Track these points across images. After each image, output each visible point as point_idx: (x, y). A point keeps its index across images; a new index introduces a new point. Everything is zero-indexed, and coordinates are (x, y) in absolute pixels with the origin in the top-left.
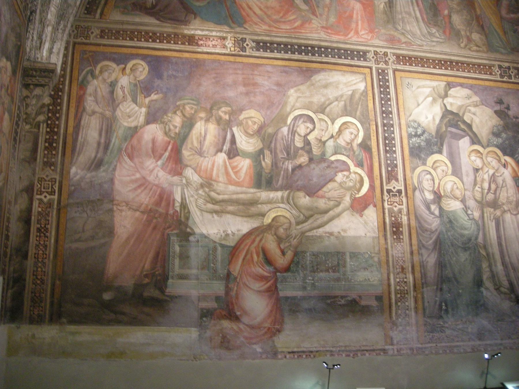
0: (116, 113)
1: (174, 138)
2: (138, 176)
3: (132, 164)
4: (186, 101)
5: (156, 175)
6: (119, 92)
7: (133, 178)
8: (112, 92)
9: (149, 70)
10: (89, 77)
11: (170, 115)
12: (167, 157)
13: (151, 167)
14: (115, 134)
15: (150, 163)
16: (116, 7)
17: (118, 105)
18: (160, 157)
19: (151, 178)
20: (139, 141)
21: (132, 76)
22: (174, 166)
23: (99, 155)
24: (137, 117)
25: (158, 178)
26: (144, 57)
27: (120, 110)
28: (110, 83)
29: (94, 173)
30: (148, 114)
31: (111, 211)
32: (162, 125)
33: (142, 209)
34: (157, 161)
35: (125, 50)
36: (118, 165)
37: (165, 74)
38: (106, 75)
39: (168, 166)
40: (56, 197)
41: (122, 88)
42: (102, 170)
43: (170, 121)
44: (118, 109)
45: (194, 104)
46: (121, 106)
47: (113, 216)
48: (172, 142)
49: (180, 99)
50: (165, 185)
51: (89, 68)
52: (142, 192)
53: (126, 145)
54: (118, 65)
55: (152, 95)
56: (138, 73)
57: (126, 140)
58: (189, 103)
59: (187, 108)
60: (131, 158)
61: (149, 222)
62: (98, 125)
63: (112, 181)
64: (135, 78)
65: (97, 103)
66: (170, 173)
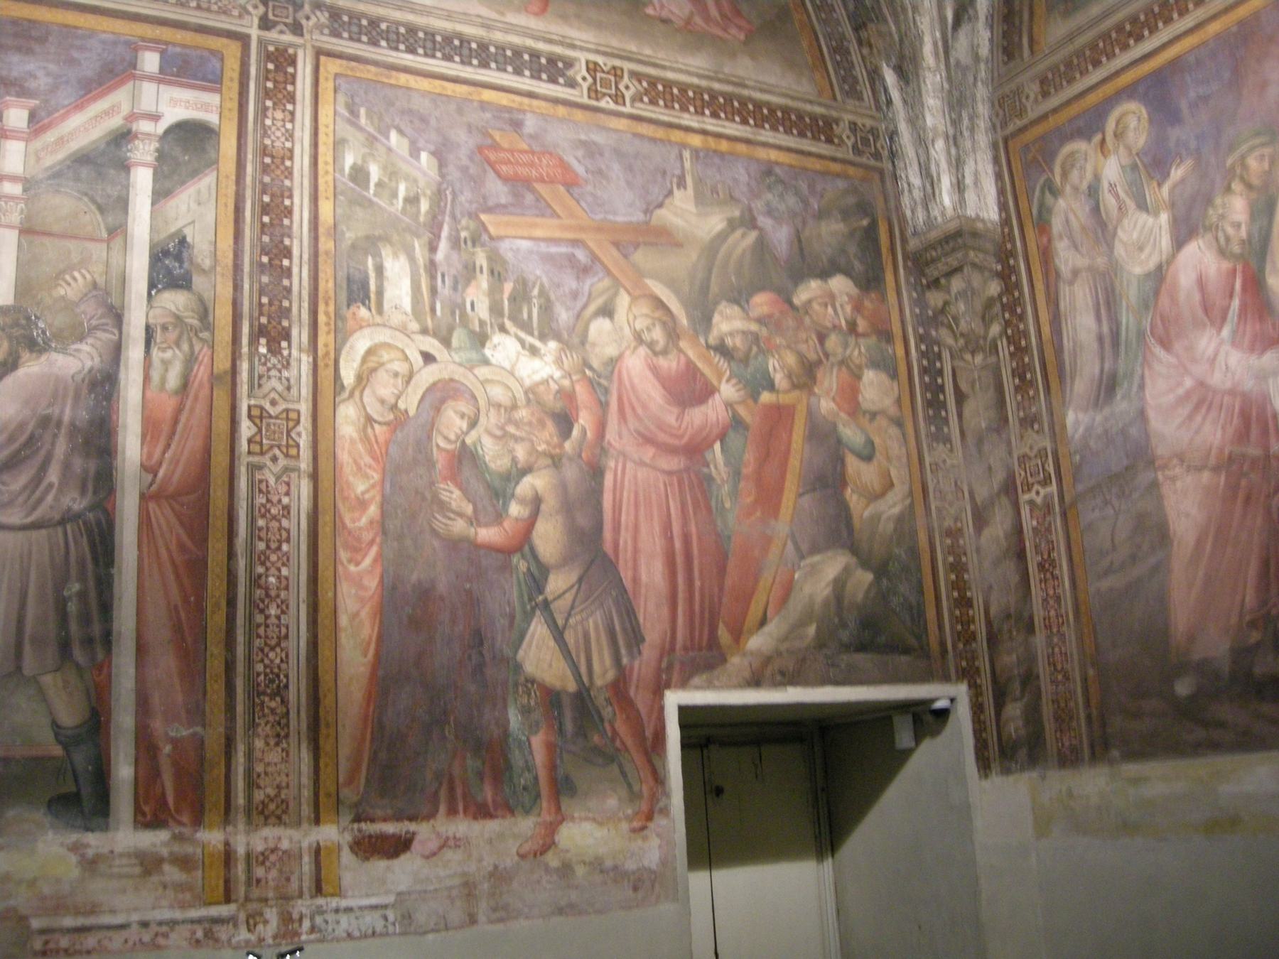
0: (1116, 253)
1: (1242, 255)
2: (1188, 383)
3: (1172, 359)
4: (1244, 148)
5: (1224, 367)
6: (1109, 201)
7: (1181, 391)
8: (1096, 210)
9: (1149, 114)
10: (1049, 198)
11: (1218, 201)
12: (1237, 310)
13: (1210, 352)
14: (1124, 303)
15: (1206, 342)
16: (1050, 9)
17: (1115, 234)
18: (1224, 319)
19: (1217, 379)
20: (1174, 300)
21: (1121, 149)
22: (1258, 326)
23: (1107, 366)
24: (1155, 240)
25: (1229, 375)
26: (1129, 92)
27: (1121, 241)
28: (1087, 192)
29: (1107, 411)
30: (1175, 223)
31: (1155, 485)
32: (1209, 236)
33: (1212, 461)
34: (1220, 329)
35: (1092, 99)
36: (1147, 373)
37: (1184, 105)
38: (1074, 175)
39: (1244, 331)
40: (1053, 488)
41: (1112, 187)
42: (1119, 397)
43: (1222, 217)
44: (1117, 243)
45: (1263, 145)
46: (1120, 233)
47: (1160, 498)
48: (1239, 268)
49: (1232, 148)
50: (1249, 385)
51: (1042, 181)
52: (1204, 419)
53: (1149, 320)
54: (1089, 139)
55: (1173, 171)
56: (1131, 135)
57: (1147, 307)
58: (1252, 149)
59: (1252, 163)
60: (1166, 344)
61: (1233, 488)
62: (1089, 299)
63: (1142, 415)
64: (1129, 149)
65: (1076, 247)
66: (1252, 349)
